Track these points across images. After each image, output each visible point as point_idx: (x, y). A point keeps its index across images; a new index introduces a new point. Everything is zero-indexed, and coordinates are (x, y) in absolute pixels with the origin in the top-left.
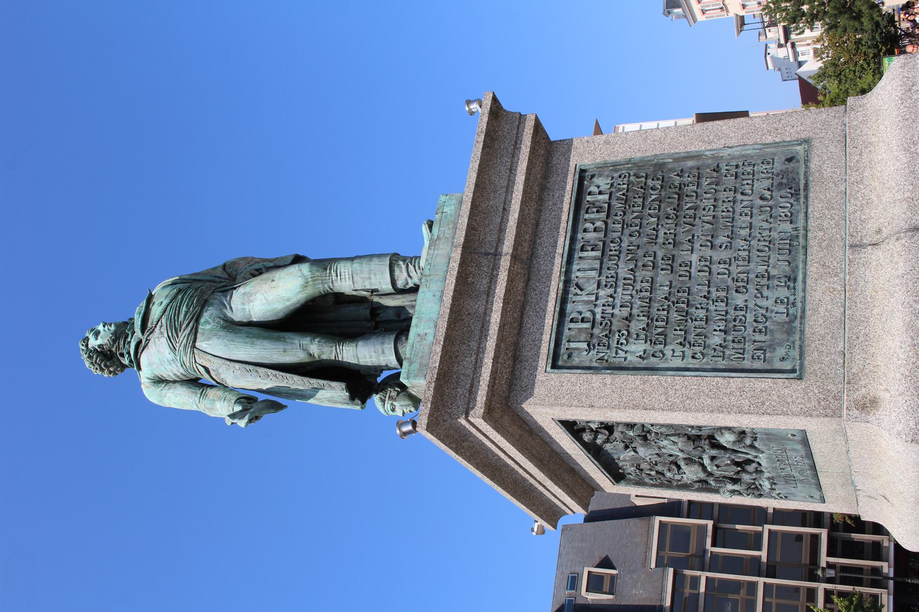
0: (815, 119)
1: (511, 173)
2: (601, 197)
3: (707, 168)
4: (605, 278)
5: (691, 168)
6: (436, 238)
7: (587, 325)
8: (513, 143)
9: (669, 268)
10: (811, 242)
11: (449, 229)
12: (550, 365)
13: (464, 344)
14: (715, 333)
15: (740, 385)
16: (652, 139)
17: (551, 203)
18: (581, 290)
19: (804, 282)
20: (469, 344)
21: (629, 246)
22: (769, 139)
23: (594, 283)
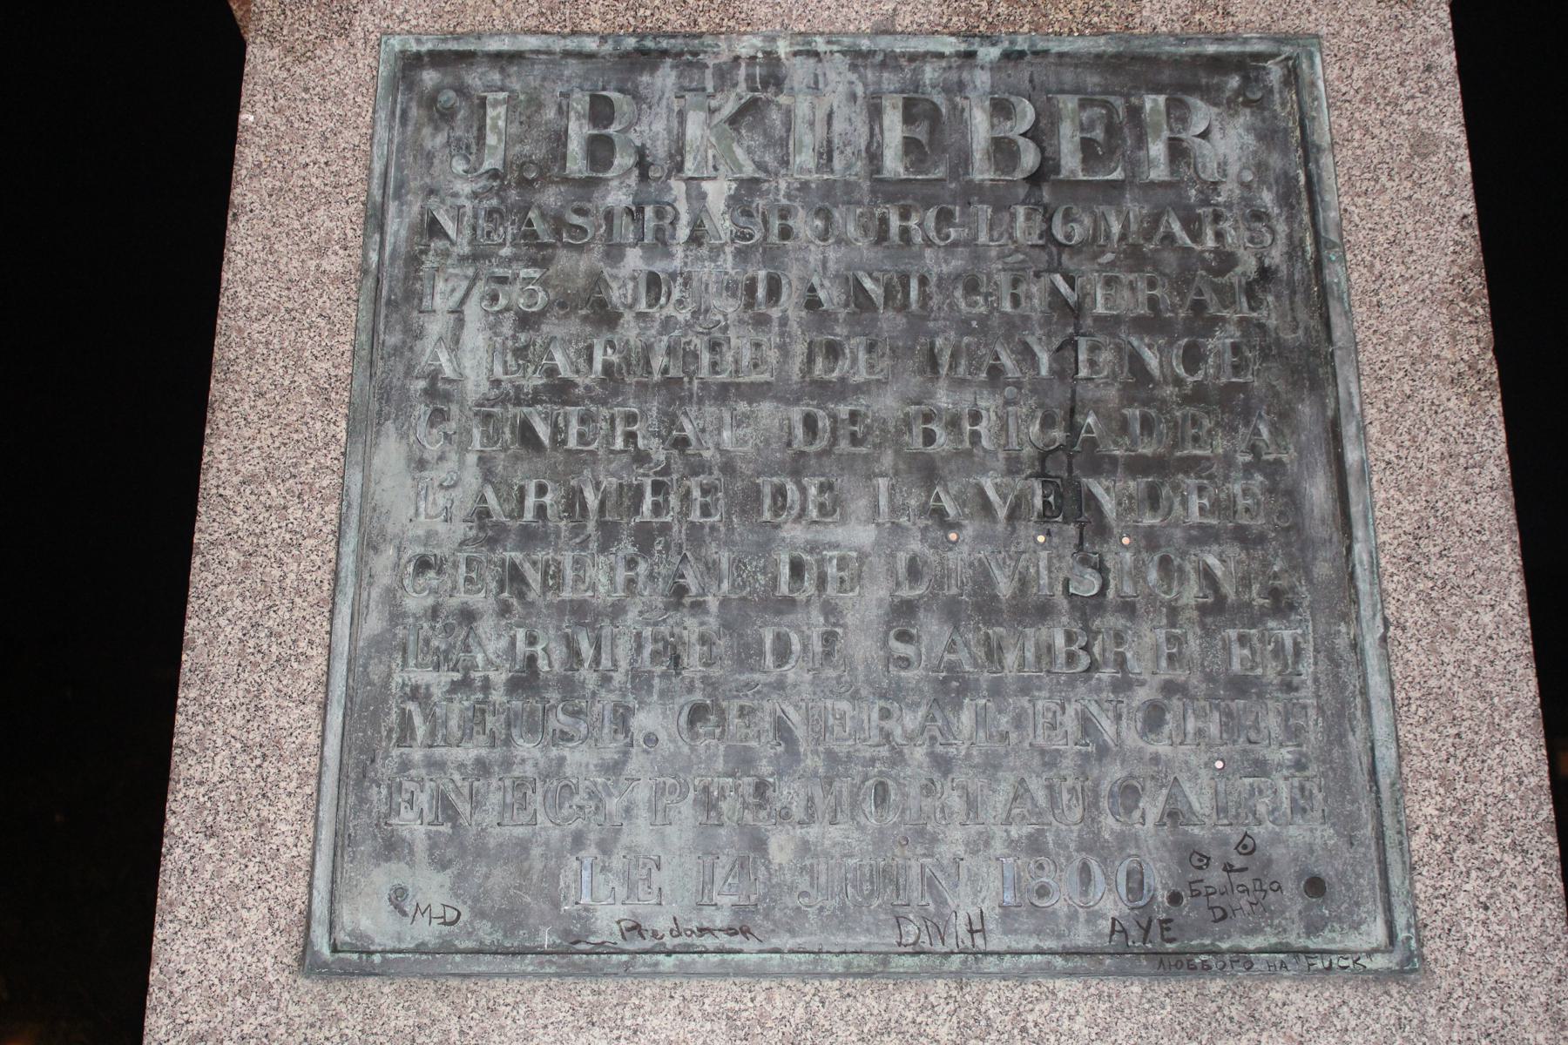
0: (1524, 999)
2: (1157, 149)
3: (1289, 557)
7: (577, 163)
9: (820, 444)
10: (903, 1001)
14: (521, 634)
15: (289, 746)
18: (734, 120)
21: (923, 281)
22: (1424, 808)
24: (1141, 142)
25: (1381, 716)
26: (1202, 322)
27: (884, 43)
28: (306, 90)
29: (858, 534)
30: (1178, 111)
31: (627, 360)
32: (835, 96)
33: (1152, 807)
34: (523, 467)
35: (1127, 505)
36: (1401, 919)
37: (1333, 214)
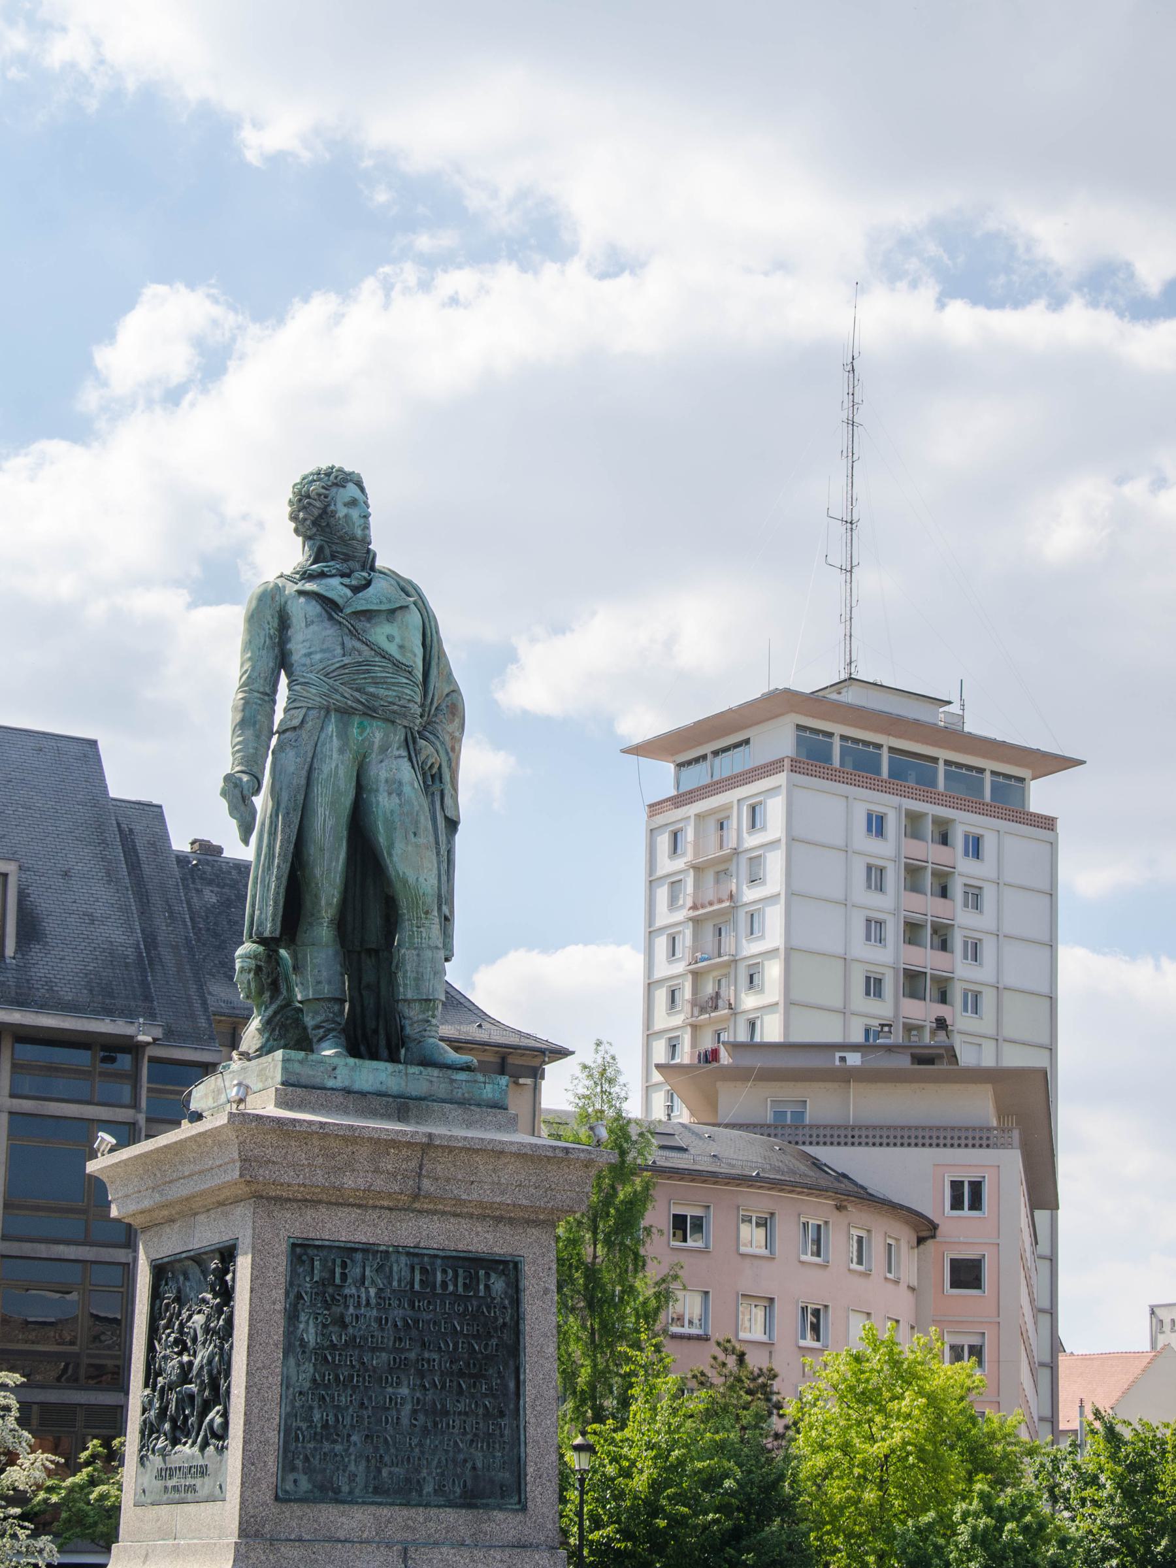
2: (482, 1287)
5: (506, 1386)
7: (338, 1281)
11: (463, 1094)
15: (271, 1441)
17: (479, 1229)
19: (372, 1503)
24: (478, 1285)
26: (489, 1336)
27: (416, 1250)
29: (404, 1391)
30: (487, 1275)
33: (469, 1465)
34: (324, 1368)
35: (469, 1387)
36: (523, 1496)
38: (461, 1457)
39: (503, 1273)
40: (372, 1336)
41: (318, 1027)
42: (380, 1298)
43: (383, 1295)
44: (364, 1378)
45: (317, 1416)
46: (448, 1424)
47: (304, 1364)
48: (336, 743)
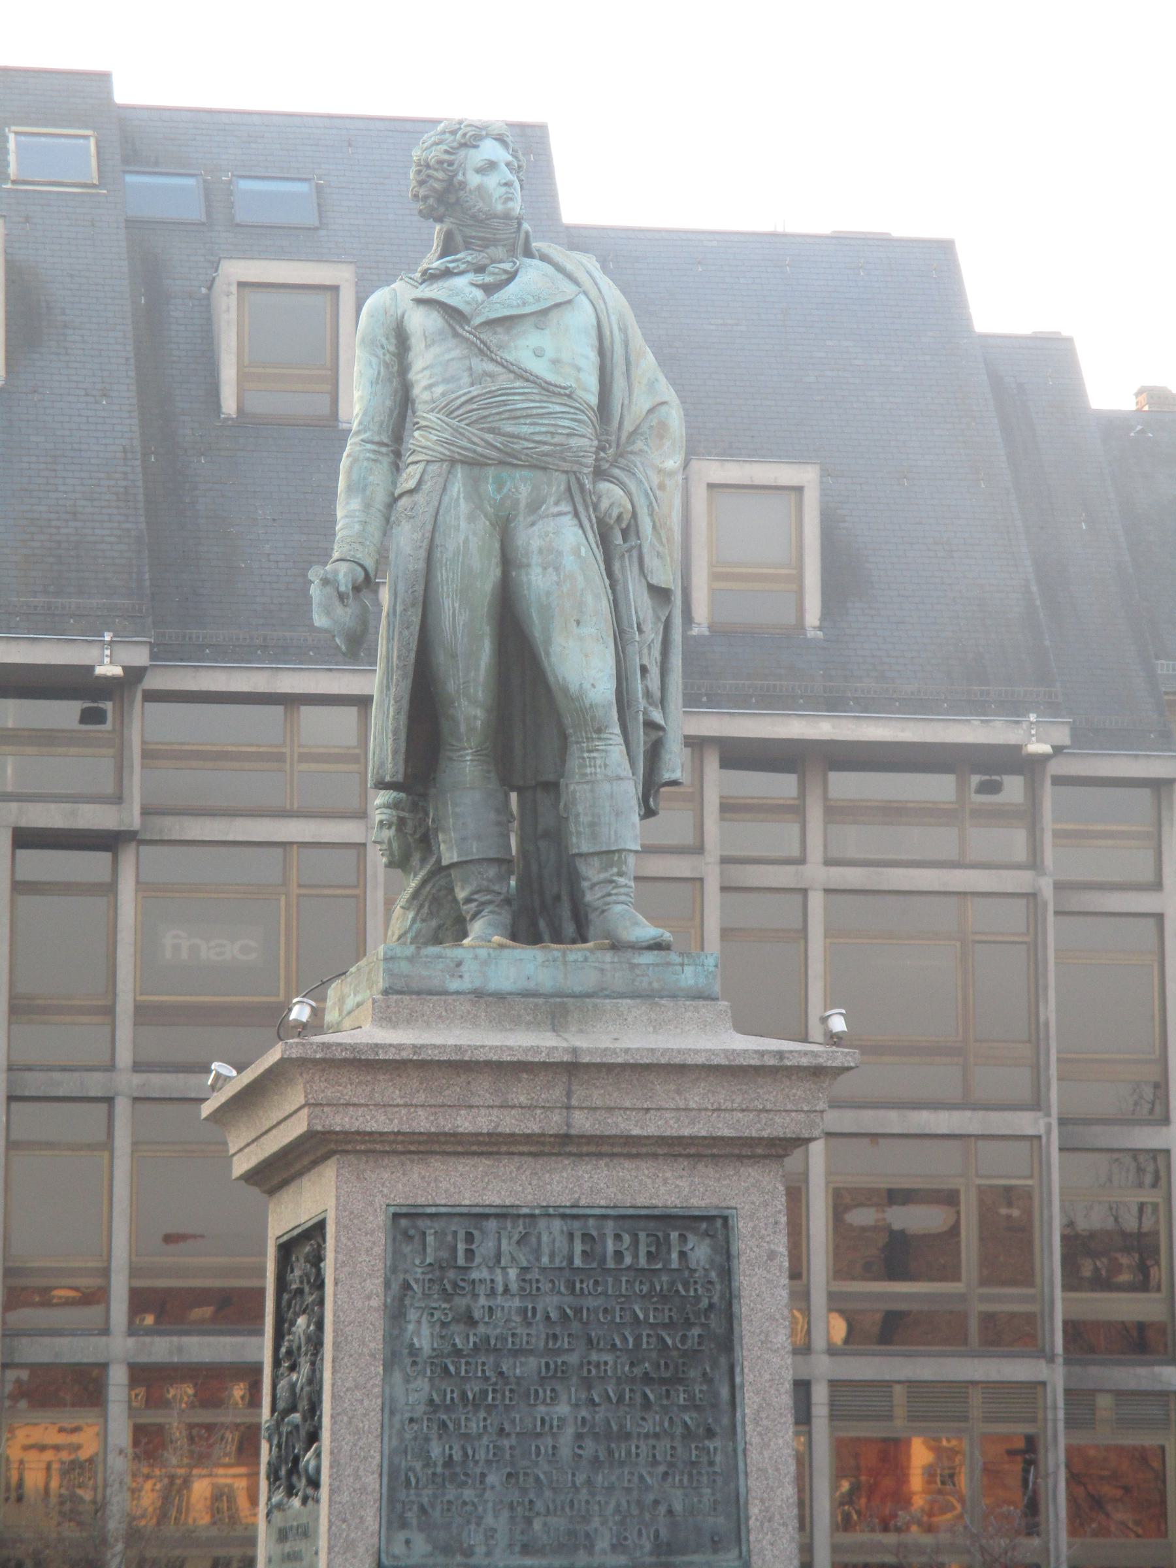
1: (714, 1110)
2: (674, 1256)
4: (537, 1277)
5: (716, 1395)
6: (635, 961)
7: (461, 1261)
8: (769, 1106)
9: (550, 1374)
11: (650, 983)
12: (398, 1210)
13: (421, 1083)
14: (447, 1447)
15: (370, 1489)
16: (770, 1329)
17: (668, 1175)
18: (518, 1242)
20: (421, 1091)
21: (588, 1309)
22: (754, 1511)
23: (528, 1261)
24: (669, 1252)
25: (742, 1477)
27: (575, 1211)
28: (360, 1230)
29: (563, 1409)
30: (683, 1238)
31: (480, 1340)
32: (556, 1233)
33: (662, 1509)
36: (744, 1549)
37: (737, 1284)
38: (650, 1497)
39: (707, 1234)
40: (513, 1335)
41: (468, 900)
42: (524, 1280)
43: (528, 1277)
44: (503, 1395)
45: (436, 1450)
46: (629, 1453)
47: (416, 1378)
48: (464, 507)
